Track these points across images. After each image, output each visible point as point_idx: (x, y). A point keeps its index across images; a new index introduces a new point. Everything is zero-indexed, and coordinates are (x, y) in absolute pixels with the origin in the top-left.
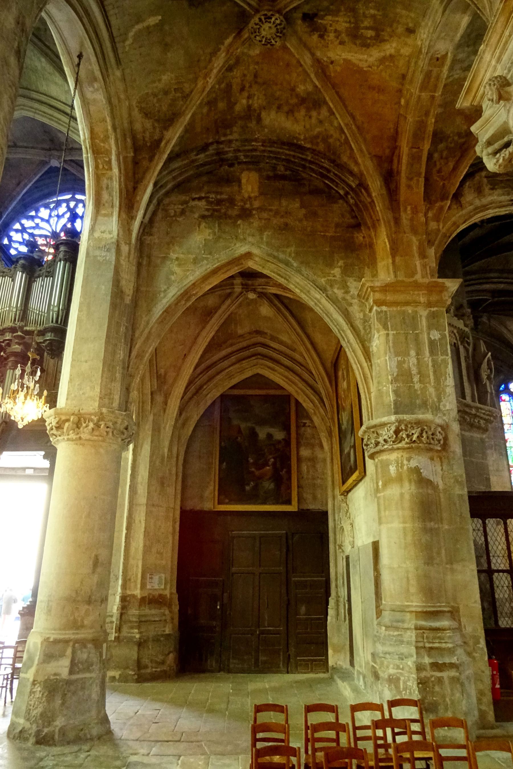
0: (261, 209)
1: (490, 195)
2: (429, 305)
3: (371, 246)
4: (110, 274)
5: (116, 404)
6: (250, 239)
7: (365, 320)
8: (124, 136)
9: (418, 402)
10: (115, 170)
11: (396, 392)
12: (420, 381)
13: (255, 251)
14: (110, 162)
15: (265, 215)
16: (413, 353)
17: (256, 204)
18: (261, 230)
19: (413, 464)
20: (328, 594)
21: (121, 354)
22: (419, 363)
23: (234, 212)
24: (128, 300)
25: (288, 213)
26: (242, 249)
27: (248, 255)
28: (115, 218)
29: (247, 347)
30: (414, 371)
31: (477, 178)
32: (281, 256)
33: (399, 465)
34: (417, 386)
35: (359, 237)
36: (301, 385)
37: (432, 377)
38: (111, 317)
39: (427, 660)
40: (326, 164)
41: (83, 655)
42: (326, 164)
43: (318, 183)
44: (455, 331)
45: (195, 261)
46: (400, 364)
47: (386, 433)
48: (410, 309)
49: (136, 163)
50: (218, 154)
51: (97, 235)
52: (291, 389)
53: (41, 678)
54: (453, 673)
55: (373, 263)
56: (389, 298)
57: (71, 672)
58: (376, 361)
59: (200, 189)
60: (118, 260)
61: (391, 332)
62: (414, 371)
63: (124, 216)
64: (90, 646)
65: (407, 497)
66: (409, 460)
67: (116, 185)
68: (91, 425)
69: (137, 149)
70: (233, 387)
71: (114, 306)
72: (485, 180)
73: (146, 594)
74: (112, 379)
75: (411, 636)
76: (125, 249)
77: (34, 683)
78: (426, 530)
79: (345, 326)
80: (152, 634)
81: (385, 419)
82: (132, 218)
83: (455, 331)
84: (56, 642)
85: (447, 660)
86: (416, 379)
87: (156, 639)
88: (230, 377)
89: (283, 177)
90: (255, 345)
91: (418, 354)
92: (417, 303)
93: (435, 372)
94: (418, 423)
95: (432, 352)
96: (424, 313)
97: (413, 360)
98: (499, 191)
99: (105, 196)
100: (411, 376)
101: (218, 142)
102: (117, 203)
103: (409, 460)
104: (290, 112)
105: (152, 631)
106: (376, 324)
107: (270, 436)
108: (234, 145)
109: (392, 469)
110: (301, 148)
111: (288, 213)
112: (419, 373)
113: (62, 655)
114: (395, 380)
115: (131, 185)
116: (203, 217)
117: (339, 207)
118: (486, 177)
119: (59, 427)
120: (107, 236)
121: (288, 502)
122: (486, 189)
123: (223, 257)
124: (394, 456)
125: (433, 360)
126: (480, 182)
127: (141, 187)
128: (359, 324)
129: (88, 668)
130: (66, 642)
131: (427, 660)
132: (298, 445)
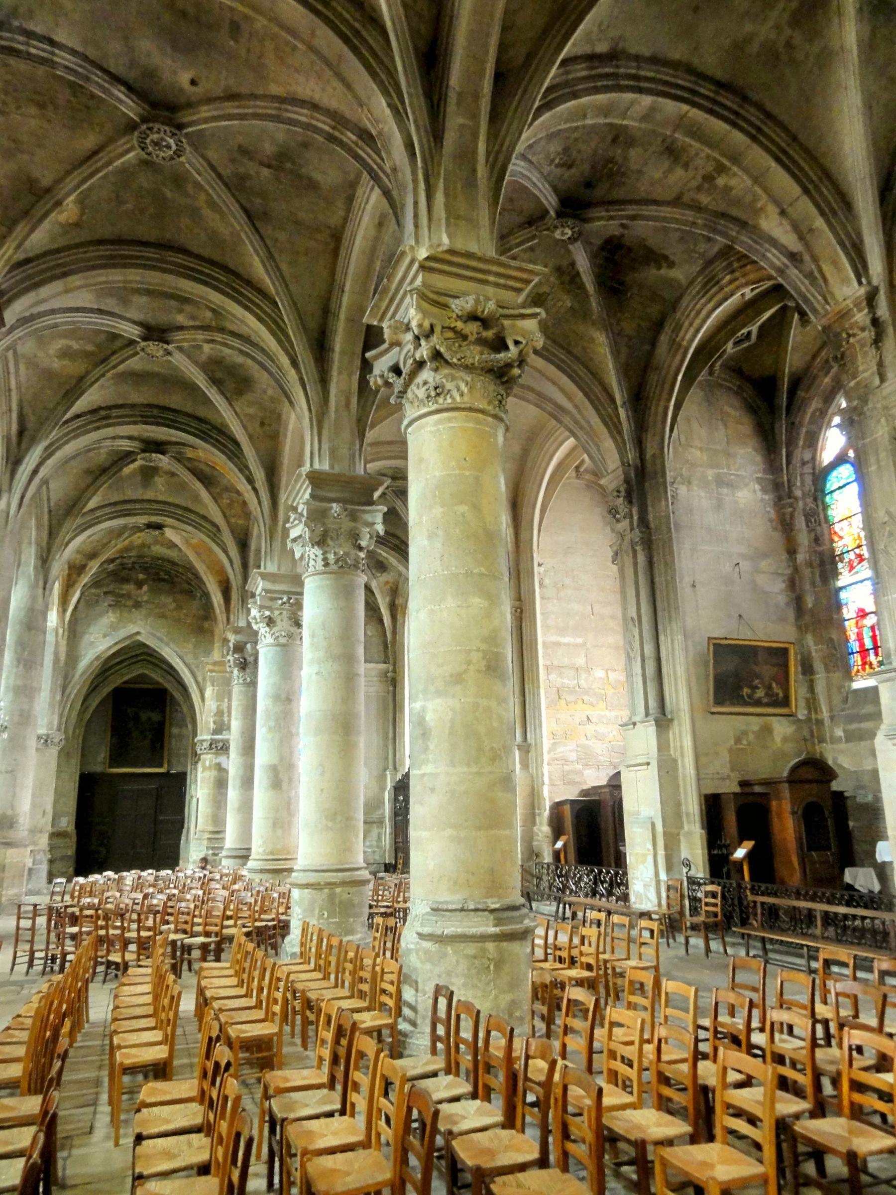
0: (147, 602)
3: (212, 632)
5: (55, 727)
6: (139, 622)
7: (204, 679)
11: (215, 723)
13: (142, 631)
15: (150, 606)
17: (145, 598)
18: (147, 617)
19: (218, 761)
20: (182, 827)
21: (58, 698)
23: (130, 603)
24: (62, 663)
25: (164, 606)
26: (132, 629)
27: (138, 633)
29: (136, 656)
30: (226, 710)
32: (158, 634)
33: (211, 761)
34: (226, 719)
35: (206, 625)
36: (175, 684)
38: (53, 676)
39: (211, 852)
40: (190, 575)
42: (190, 575)
43: (185, 586)
45: (105, 636)
46: (218, 706)
47: (206, 745)
49: (69, 575)
50: (122, 564)
52: (167, 686)
55: (212, 642)
56: (217, 668)
58: (207, 703)
59: (108, 585)
60: (57, 641)
62: (226, 710)
69: (70, 568)
70: (124, 683)
73: (55, 830)
75: (205, 843)
76: (61, 631)
79: (192, 681)
80: (59, 855)
81: (205, 737)
82: (64, 611)
86: (226, 715)
87: (63, 858)
88: (122, 675)
89: (163, 580)
90: (142, 654)
94: (222, 740)
97: (225, 705)
101: (123, 557)
104: (169, 548)
105: (59, 853)
106: (208, 683)
107: (149, 719)
108: (132, 559)
109: (207, 763)
110: (177, 564)
111: (164, 606)
114: (215, 715)
116: (110, 605)
117: (196, 604)
121: (161, 766)
123: (122, 633)
124: (210, 756)
127: (71, 591)
128: (200, 679)
131: (211, 852)
132: (171, 724)
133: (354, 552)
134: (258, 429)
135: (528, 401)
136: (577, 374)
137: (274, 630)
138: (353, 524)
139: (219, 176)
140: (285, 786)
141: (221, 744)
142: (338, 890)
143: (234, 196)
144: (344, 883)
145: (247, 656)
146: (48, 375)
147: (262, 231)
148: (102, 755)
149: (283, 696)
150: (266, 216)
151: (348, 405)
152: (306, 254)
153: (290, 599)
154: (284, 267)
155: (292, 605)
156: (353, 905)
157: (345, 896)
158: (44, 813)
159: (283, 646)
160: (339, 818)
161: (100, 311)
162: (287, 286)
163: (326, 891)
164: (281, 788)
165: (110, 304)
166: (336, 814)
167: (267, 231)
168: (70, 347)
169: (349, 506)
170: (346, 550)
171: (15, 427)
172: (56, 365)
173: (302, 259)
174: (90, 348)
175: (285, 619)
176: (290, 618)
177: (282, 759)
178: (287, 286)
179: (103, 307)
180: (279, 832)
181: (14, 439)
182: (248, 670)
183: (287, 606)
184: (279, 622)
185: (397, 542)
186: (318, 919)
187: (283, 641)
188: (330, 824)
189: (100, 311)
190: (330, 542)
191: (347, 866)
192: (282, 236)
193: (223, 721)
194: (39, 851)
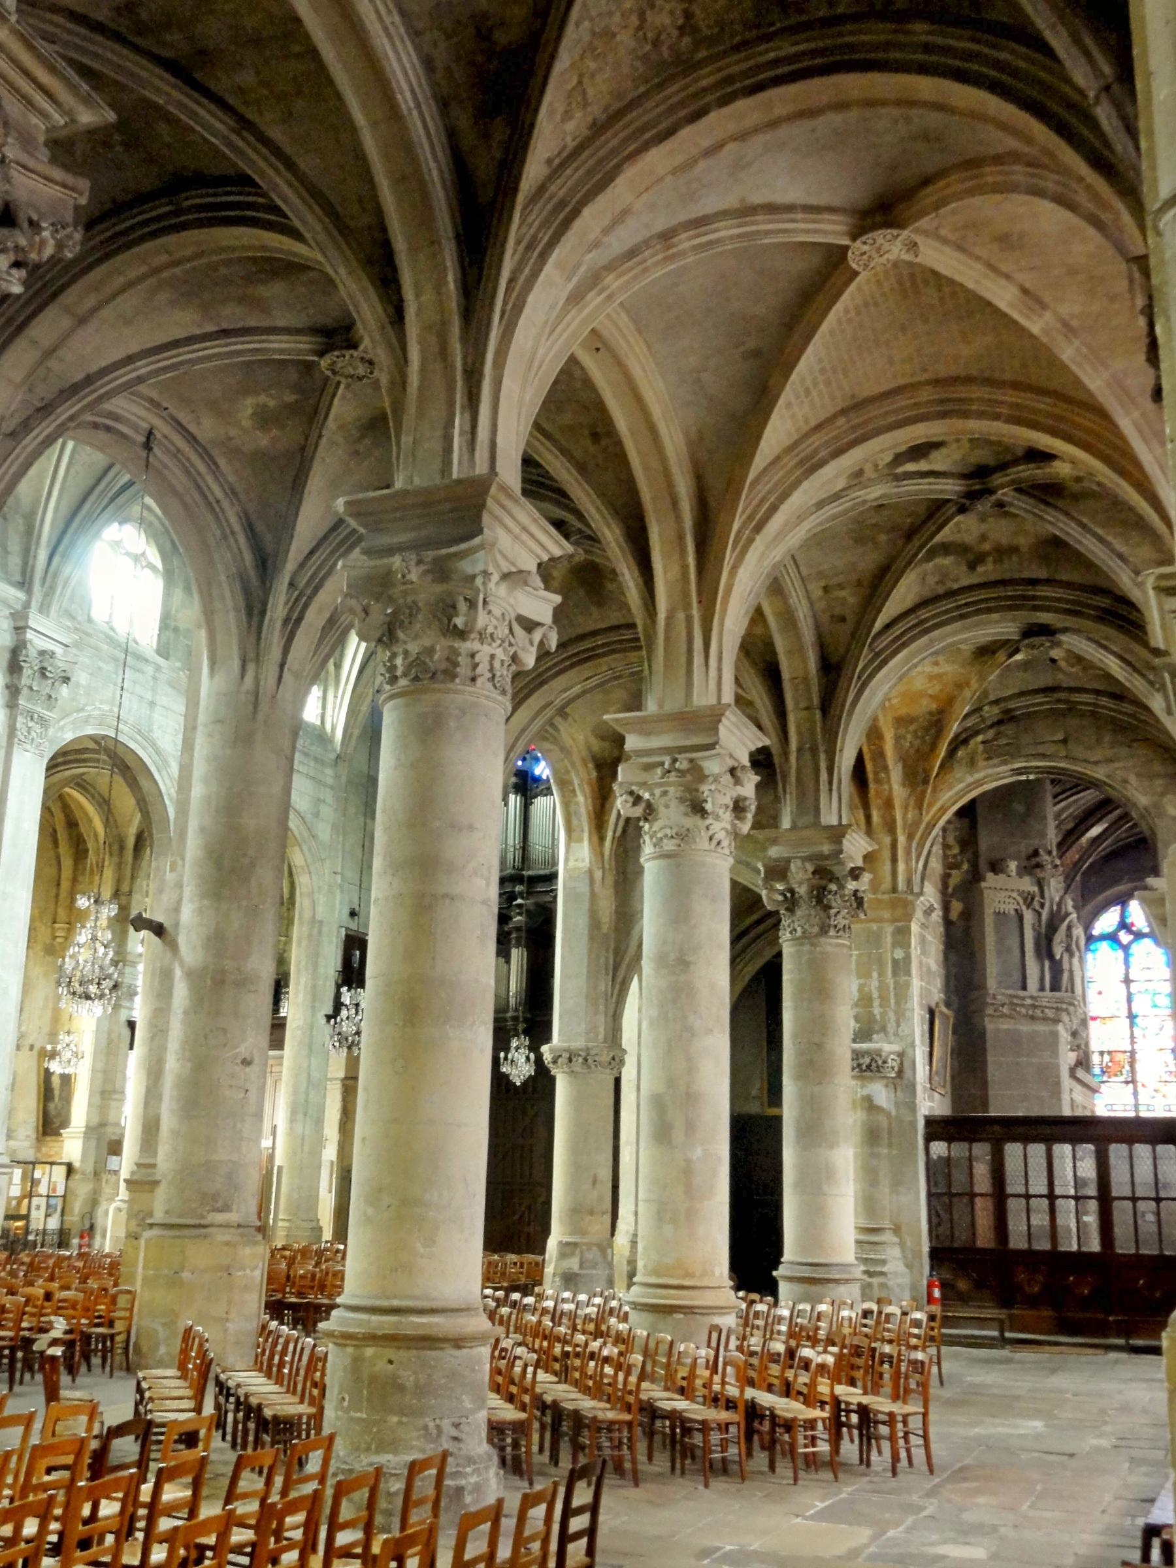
1: (986, 767)
2: (894, 920)
4: (586, 906)
8: (584, 762)
9: (877, 1028)
10: (580, 798)
12: (881, 1006)
14: (574, 791)
16: (875, 975)
19: (865, 1092)
22: (882, 988)
24: (605, 929)
28: (586, 843)
30: (875, 995)
31: (972, 743)
34: (877, 1011)
37: (892, 1001)
38: (590, 951)
41: (589, 1256)
44: (1015, 895)
46: (861, 988)
48: (875, 926)
51: (571, 864)
53: (559, 1271)
54: (882, 1279)
57: (581, 1267)
61: (855, 952)
62: (875, 995)
63: (595, 839)
64: (595, 1248)
65: (859, 1124)
66: (862, 1087)
67: (583, 811)
68: (580, 1060)
69: (599, 766)
71: (592, 938)
72: (981, 747)
74: (596, 1013)
76: (598, 874)
77: (554, 1275)
78: (873, 1155)
82: (602, 839)
83: (1015, 895)
84: (568, 1244)
85: (878, 1269)
86: (876, 1003)
91: (880, 975)
92: (880, 920)
93: (896, 995)
95: (895, 973)
96: (889, 929)
97: (874, 984)
98: (995, 761)
99: (575, 822)
100: (870, 999)
102: (586, 828)
103: (862, 1087)
112: (880, 997)
113: (572, 1254)
114: (856, 1005)
115: (598, 802)
118: (983, 742)
119: (555, 1062)
120: (580, 865)
122: (981, 763)
125: (896, 984)
126: (974, 752)
129: (594, 1266)
130: (575, 1245)
133: (441, 647)
134: (592, 449)
135: (1013, 188)
136: (1015, 73)
137: (656, 826)
138: (439, 588)
139: (98, 27)
140: (678, 1135)
141: (867, 1060)
142: (369, 1352)
143: (137, 49)
144: (373, 1338)
145: (795, 886)
146: (260, 460)
147: (212, 86)
148: (758, 1085)
149: (672, 956)
150: (204, 55)
151: (443, 352)
152: (299, 93)
153: (675, 760)
154: (276, 134)
155: (682, 773)
156: (401, 1388)
157: (381, 1366)
158: (595, 1182)
159: (667, 856)
160: (386, 1200)
161: (225, 333)
162: (290, 165)
163: (350, 1350)
164: (670, 1143)
165: (232, 315)
166: (380, 1190)
167: (222, 84)
168: (265, 406)
169: (430, 555)
170: (427, 642)
171: (248, 558)
172: (263, 441)
173: (299, 104)
174: (290, 398)
175: (674, 804)
176: (682, 800)
177: (671, 1083)
178: (290, 165)
179: (225, 326)
180: (668, 1230)
181: (252, 574)
182: (799, 913)
183: (672, 777)
184: (662, 810)
185: (1104, 602)
186: (336, 1410)
187: (669, 846)
188: (370, 1211)
189: (225, 333)
190: (400, 634)
191: (396, 1303)
192: (247, 78)
193: (871, 1014)
194: (590, 1245)
